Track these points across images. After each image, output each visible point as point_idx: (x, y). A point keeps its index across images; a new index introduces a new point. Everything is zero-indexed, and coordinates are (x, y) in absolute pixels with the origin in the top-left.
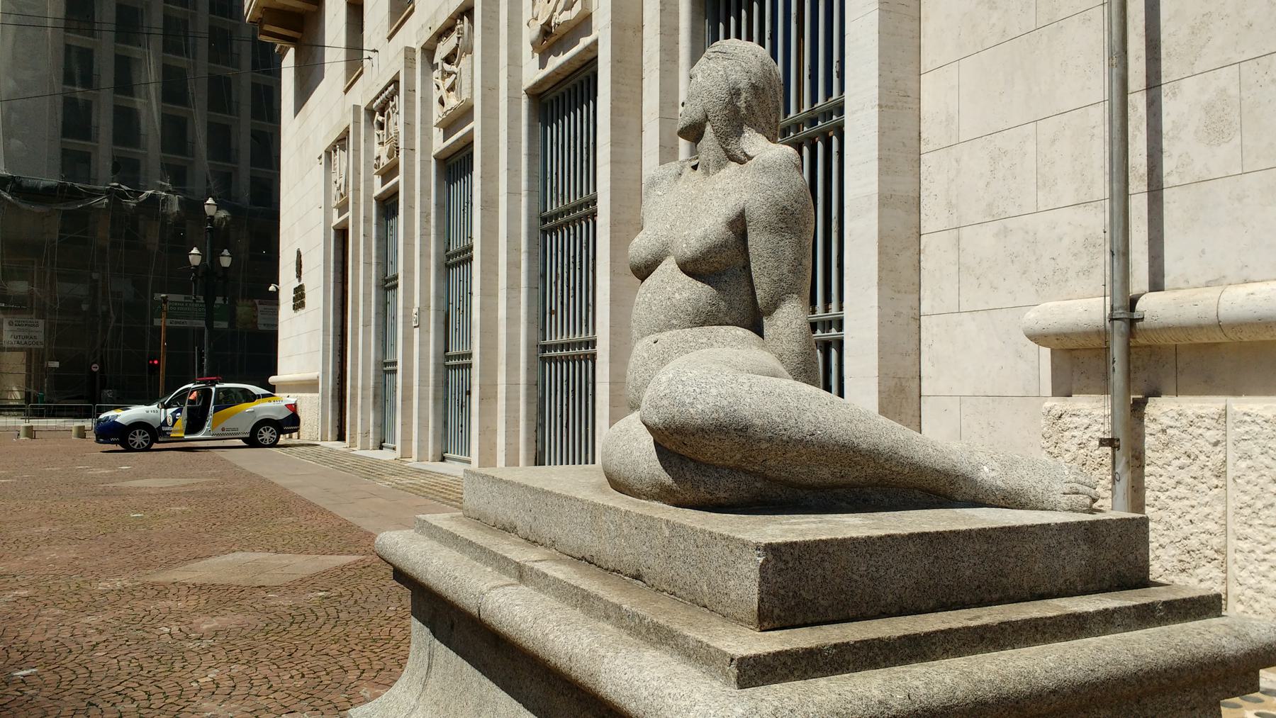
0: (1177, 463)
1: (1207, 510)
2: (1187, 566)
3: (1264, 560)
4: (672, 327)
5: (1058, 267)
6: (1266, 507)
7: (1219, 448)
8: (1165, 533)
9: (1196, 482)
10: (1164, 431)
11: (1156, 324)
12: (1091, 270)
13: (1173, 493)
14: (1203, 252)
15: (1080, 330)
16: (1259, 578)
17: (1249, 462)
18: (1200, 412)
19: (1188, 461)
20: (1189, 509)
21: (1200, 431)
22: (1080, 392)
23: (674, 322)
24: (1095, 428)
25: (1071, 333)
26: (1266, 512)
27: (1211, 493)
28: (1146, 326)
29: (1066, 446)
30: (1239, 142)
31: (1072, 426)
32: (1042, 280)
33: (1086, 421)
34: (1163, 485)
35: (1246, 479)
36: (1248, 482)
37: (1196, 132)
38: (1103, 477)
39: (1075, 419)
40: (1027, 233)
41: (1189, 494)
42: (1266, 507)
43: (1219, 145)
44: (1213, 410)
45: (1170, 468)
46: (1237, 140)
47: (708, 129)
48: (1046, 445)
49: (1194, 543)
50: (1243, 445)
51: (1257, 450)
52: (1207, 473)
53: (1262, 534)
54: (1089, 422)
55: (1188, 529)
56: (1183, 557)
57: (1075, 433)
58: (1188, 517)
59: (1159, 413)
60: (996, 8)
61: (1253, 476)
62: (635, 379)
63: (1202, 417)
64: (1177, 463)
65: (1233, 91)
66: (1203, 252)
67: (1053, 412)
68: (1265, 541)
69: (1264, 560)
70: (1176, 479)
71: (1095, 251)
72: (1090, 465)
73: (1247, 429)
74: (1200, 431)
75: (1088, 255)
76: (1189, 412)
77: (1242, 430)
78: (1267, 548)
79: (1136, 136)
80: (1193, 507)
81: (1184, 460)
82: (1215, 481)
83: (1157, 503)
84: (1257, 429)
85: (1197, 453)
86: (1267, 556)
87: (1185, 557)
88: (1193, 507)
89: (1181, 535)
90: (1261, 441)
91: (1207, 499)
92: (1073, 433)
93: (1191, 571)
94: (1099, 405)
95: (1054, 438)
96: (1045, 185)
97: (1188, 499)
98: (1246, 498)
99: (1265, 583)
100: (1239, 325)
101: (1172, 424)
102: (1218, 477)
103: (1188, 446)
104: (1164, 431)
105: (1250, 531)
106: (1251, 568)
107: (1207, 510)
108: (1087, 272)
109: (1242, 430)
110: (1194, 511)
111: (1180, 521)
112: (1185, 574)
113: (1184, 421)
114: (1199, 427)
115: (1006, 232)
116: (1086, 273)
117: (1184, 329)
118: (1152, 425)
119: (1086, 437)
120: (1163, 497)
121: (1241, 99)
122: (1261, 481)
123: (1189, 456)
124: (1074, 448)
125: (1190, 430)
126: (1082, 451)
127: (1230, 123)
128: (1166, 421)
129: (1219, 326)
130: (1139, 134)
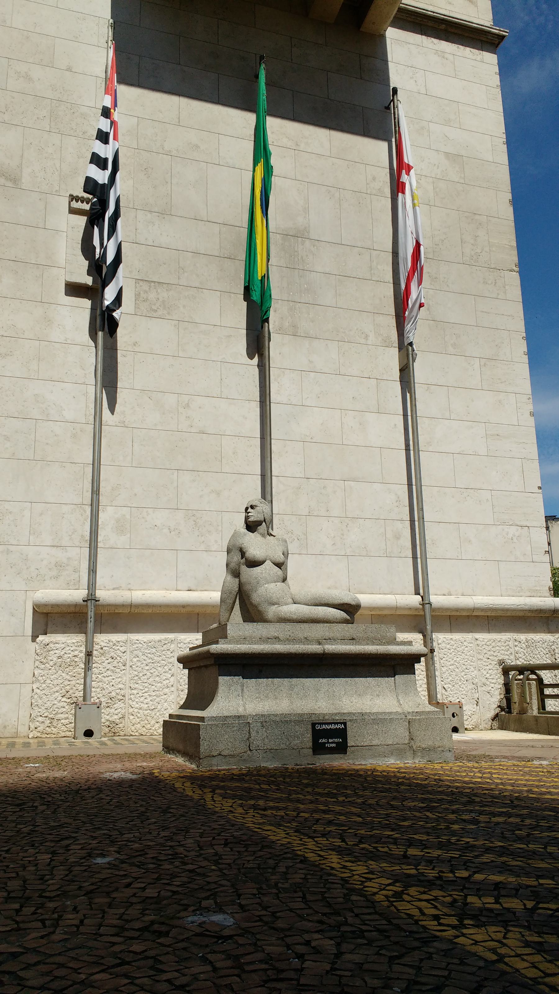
0: (107, 661)
1: (120, 680)
2: (110, 704)
3: (142, 696)
4: (278, 582)
5: (39, 573)
6: (143, 675)
7: (125, 654)
8: (101, 692)
9: (115, 669)
10: (102, 648)
11: (105, 603)
12: (58, 577)
13: (105, 674)
14: (112, 576)
15: (67, 603)
16: (140, 704)
17: (138, 659)
18: (118, 640)
19: (112, 660)
20: (112, 680)
21: (118, 648)
22: (52, 633)
23: (279, 580)
24: (68, 649)
25: (62, 605)
26: (144, 677)
27: (121, 672)
28: (100, 604)
29: (51, 658)
30: (129, 537)
31: (55, 648)
32: (29, 578)
33: (63, 646)
34: (101, 672)
35: (136, 665)
36: (137, 666)
37: (112, 528)
38: (71, 671)
39: (56, 645)
40: (22, 554)
41: (112, 674)
42: (143, 675)
43: (121, 536)
44: (124, 639)
45: (104, 664)
46: (128, 535)
47: (264, 523)
48: (39, 658)
49: (113, 694)
50: (135, 652)
51: (141, 654)
52: (120, 664)
53: (142, 686)
54: (64, 646)
55: (111, 689)
56: (108, 701)
57: (56, 651)
58: (111, 684)
59: (100, 641)
60: (9, 441)
61: (139, 664)
62: (276, 596)
63: (119, 642)
64: (107, 661)
65: (128, 517)
66: (112, 576)
67: (44, 642)
68: (142, 688)
69: (142, 696)
70: (107, 668)
71: (62, 568)
72: (64, 666)
73: (137, 646)
74: (118, 648)
75: (57, 570)
76: (114, 640)
77: (135, 646)
78: (143, 691)
79: (85, 523)
80: (113, 679)
81: (110, 660)
82: (124, 668)
83: (97, 680)
84: (141, 645)
85: (117, 656)
86: (143, 695)
87: (110, 701)
88: (113, 679)
89: (107, 692)
90: (142, 650)
91: (120, 675)
92: (55, 652)
93: (112, 706)
94: (69, 638)
95: (44, 655)
96: (34, 533)
97: (111, 676)
98: (136, 673)
99: (142, 705)
100: (138, 606)
101: (106, 645)
102: (124, 666)
103: (112, 654)
104: (102, 648)
105: (137, 685)
106: (137, 700)
107: (120, 680)
108: (56, 577)
109: (135, 646)
110: (114, 681)
111: (107, 686)
112: (109, 708)
113: (111, 644)
114: (118, 646)
115: (8, 552)
116: (56, 578)
117: (116, 606)
118: (96, 646)
119: (63, 653)
120: (100, 677)
121: (131, 521)
122: (142, 666)
123: (113, 658)
124: (55, 659)
125: (113, 647)
126: (59, 660)
127: (126, 529)
128: (103, 644)
129: (131, 606)
130: (86, 523)
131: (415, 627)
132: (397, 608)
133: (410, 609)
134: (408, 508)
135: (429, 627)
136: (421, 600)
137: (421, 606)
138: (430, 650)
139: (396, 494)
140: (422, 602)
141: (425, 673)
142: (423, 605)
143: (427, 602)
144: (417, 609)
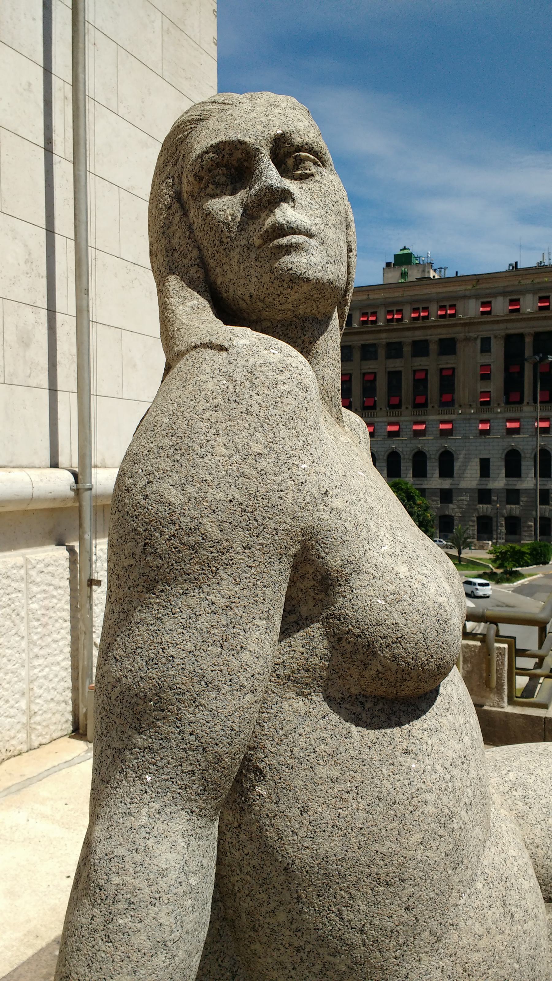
131: (51, 532)
132: (32, 499)
133: (54, 499)
134: (44, 281)
135: (87, 537)
136: (72, 479)
137: (72, 494)
138: (88, 581)
139: (26, 246)
140: (74, 484)
141: (68, 624)
142: (77, 491)
143: (87, 486)
144: (65, 499)
